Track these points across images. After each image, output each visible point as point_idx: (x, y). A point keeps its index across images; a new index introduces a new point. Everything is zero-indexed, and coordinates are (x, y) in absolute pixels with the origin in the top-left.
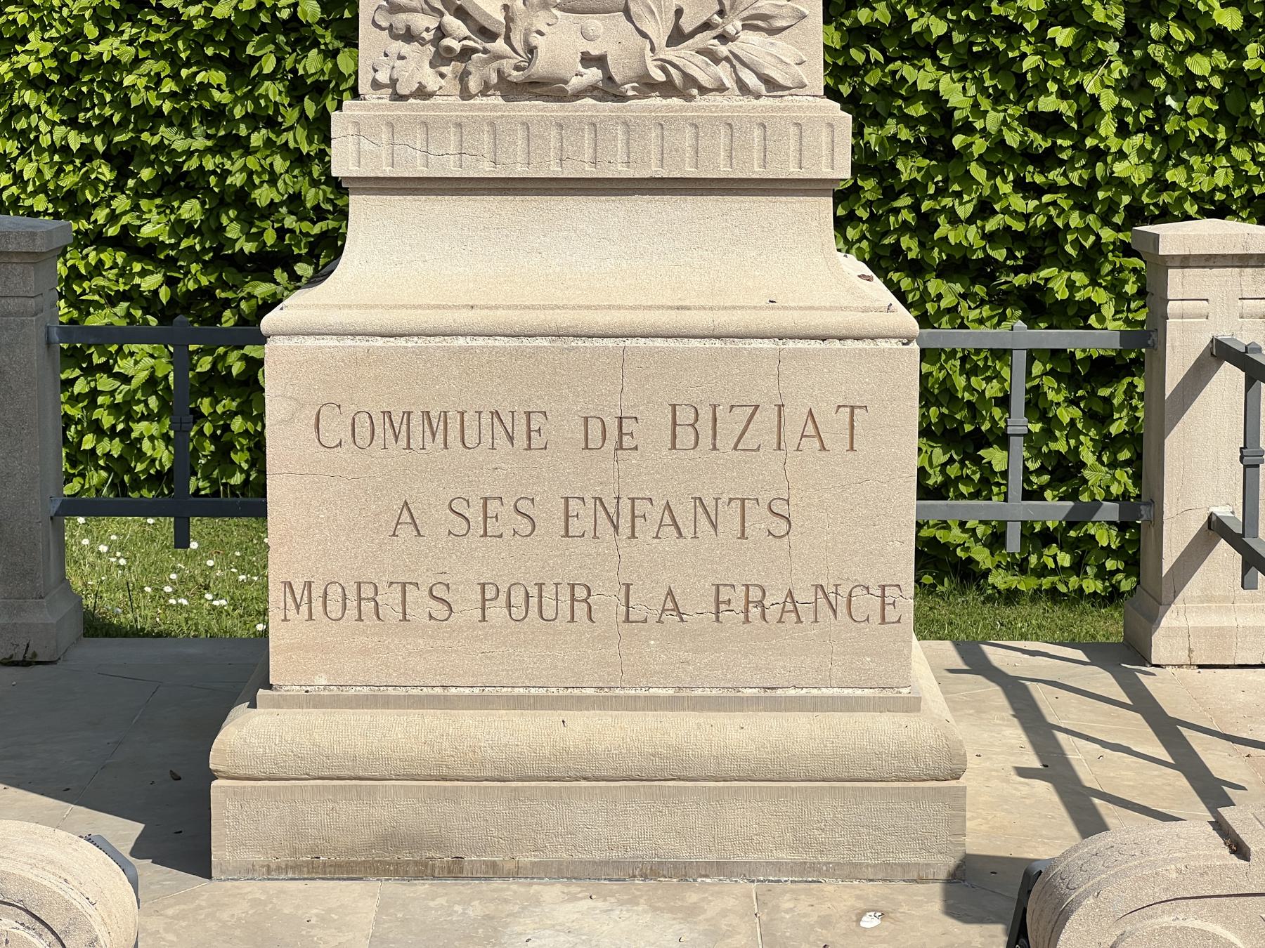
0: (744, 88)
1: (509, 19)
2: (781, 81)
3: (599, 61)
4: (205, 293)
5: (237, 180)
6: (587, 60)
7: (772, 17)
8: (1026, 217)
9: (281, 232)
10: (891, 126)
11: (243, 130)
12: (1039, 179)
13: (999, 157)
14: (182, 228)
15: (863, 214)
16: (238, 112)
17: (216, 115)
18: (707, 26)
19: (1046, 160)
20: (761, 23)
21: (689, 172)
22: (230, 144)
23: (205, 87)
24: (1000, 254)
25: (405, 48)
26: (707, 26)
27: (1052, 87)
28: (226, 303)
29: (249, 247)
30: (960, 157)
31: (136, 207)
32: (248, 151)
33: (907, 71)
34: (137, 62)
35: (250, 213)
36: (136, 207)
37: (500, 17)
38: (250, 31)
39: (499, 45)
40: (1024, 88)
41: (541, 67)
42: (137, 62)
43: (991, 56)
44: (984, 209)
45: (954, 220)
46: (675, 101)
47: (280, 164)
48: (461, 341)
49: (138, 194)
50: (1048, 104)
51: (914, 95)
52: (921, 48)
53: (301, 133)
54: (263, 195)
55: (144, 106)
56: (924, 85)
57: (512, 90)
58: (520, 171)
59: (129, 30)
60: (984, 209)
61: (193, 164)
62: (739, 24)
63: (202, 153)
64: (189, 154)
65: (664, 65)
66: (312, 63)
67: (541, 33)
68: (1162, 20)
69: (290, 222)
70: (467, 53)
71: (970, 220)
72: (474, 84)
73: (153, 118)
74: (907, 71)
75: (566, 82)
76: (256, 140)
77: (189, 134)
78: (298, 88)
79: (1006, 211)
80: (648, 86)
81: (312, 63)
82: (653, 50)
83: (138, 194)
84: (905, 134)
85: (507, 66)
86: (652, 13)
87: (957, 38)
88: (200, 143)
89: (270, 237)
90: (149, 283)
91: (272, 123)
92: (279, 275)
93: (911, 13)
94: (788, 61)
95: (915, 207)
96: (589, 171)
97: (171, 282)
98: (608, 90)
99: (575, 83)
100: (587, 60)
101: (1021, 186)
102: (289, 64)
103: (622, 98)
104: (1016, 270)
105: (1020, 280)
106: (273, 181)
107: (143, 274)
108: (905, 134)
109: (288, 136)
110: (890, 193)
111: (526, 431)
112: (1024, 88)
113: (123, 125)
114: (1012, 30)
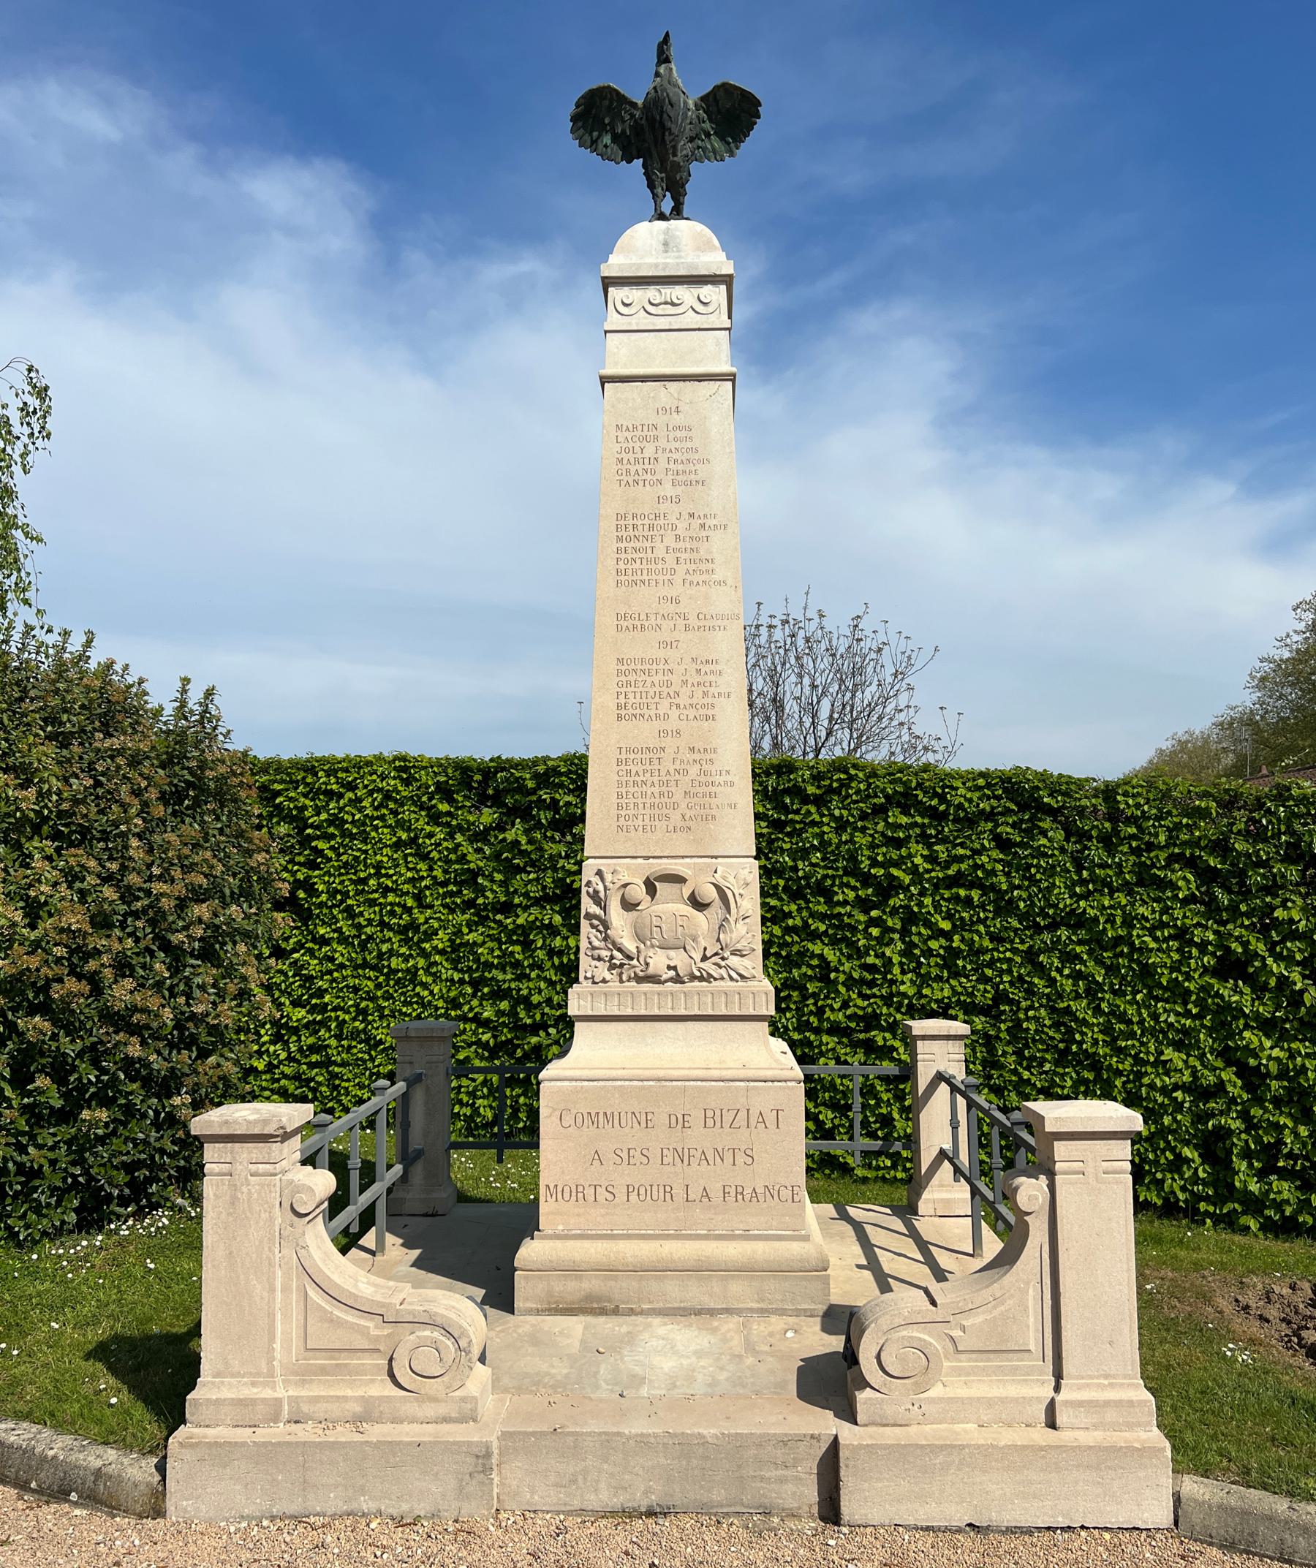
0: (731, 978)
1: (639, 952)
3: (675, 968)
4: (509, 1041)
5: (525, 992)
6: (669, 968)
8: (864, 1009)
9: (543, 1014)
10: (804, 969)
11: (528, 971)
12: (869, 992)
13: (850, 983)
14: (500, 1013)
15: (793, 1006)
16: (526, 963)
17: (517, 964)
18: (716, 954)
19: (871, 984)
21: (710, 1012)
22: (522, 977)
23: (512, 953)
24: (853, 1025)
25: (596, 963)
26: (716, 954)
27: (872, 953)
28: (518, 1046)
29: (529, 1021)
30: (835, 982)
31: (481, 1004)
32: (530, 980)
33: (810, 946)
34: (484, 943)
35: (530, 1007)
36: (481, 1004)
37: (635, 951)
38: (531, 929)
39: (635, 962)
40: (861, 954)
41: (651, 971)
42: (484, 943)
43: (845, 939)
44: (845, 1005)
45: (832, 1009)
46: (704, 984)
47: (543, 985)
48: (619, 1083)
49: (482, 999)
50: (870, 960)
51: (813, 956)
52: (815, 936)
53: (552, 972)
54: (536, 999)
55: (487, 961)
56: (817, 952)
57: (639, 980)
58: (643, 1012)
59: (481, 929)
60: (845, 1005)
61: (506, 985)
63: (510, 981)
64: (505, 981)
66: (558, 942)
68: (917, 926)
69: (547, 1010)
70: (622, 965)
71: (840, 1010)
72: (624, 978)
73: (489, 966)
74: (810, 946)
76: (533, 975)
77: (505, 973)
78: (551, 953)
79: (855, 1006)
80: (693, 978)
81: (558, 942)
83: (482, 999)
84: (810, 973)
85: (638, 970)
87: (830, 932)
88: (509, 976)
89: (538, 1017)
90: (485, 1038)
91: (541, 968)
92: (542, 1033)
93: (810, 921)
95: (815, 1004)
96: (670, 1012)
97: (495, 1037)
98: (678, 979)
99: (664, 977)
100: (669, 968)
101: (860, 995)
102: (548, 942)
104: (861, 1032)
105: (862, 1036)
106: (540, 992)
107: (483, 1033)
108: (810, 973)
109: (547, 973)
110: (805, 997)
111: (646, 1121)
112: (861, 954)
113: (477, 969)
114: (853, 929)
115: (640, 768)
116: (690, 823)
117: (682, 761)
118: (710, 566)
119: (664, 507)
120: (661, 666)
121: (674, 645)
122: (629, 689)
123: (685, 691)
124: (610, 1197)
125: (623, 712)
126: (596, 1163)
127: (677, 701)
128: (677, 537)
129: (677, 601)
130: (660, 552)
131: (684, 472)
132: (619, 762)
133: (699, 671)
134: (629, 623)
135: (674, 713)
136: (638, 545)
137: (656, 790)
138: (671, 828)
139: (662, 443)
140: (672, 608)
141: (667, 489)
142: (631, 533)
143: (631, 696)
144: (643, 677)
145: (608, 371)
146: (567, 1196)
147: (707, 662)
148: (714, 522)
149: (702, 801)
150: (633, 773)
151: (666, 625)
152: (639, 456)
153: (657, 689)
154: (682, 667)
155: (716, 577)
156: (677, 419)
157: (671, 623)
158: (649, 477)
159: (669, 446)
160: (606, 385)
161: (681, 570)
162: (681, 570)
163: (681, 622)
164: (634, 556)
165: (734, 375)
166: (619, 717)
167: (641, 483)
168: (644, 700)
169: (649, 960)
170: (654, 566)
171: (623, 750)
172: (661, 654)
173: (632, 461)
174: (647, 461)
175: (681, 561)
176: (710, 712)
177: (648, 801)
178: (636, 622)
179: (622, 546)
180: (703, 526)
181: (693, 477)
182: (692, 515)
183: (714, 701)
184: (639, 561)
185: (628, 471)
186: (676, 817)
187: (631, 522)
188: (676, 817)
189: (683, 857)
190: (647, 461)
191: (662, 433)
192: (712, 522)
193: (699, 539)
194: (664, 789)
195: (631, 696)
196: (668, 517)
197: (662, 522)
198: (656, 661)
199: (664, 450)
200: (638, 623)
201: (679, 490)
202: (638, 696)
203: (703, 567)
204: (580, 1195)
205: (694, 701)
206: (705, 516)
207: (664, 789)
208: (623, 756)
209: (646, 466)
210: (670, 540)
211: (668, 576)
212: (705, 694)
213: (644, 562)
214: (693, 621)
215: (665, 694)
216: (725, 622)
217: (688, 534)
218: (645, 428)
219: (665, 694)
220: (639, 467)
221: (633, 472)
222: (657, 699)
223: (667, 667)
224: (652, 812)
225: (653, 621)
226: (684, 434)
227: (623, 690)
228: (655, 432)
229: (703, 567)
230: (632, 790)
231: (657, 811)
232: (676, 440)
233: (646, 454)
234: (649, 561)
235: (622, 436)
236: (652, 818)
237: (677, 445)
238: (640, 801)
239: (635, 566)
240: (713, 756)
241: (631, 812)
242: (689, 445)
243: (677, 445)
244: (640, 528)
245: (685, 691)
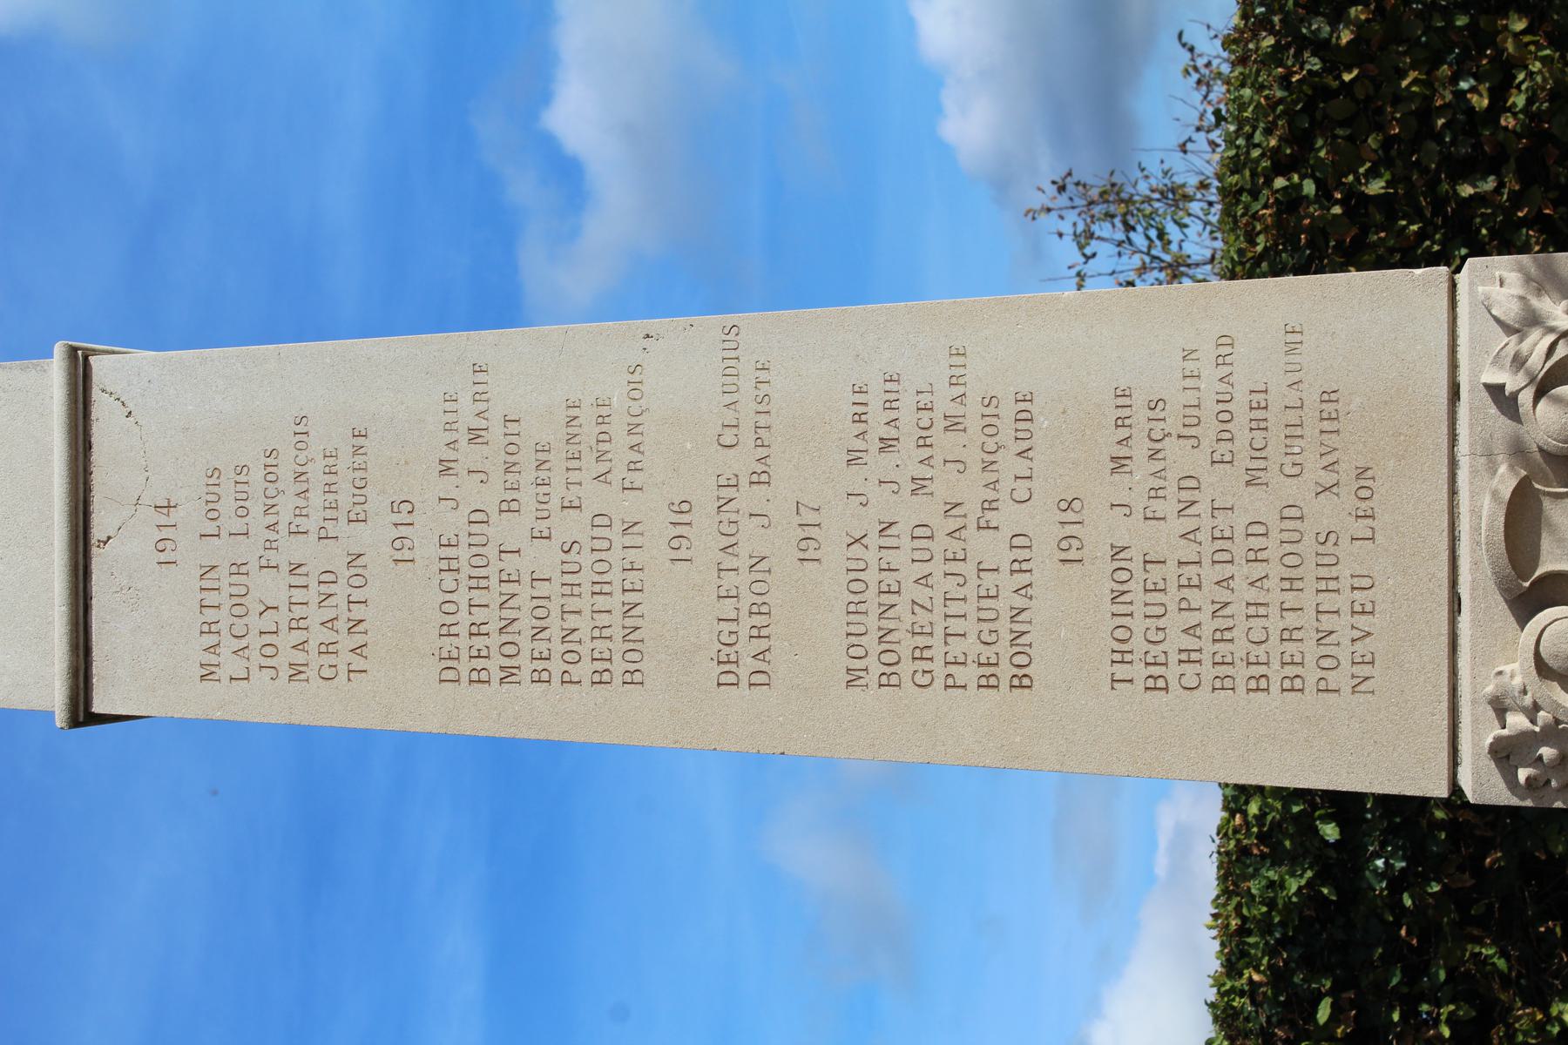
115: (1176, 621)
116: (1346, 471)
117: (1155, 494)
118: (587, 415)
119: (426, 551)
120: (872, 556)
121: (810, 517)
122: (938, 652)
123: (945, 485)
125: (1005, 671)
127: (972, 509)
128: (509, 508)
129: (682, 507)
130: (546, 559)
131: (329, 488)
132: (1156, 685)
133: (886, 444)
134: (747, 648)
135: (1009, 517)
136: (526, 623)
137: (1242, 571)
138: (1361, 528)
139: (249, 551)
140: (704, 524)
141: (374, 537)
142: (495, 640)
143: (957, 648)
144: (903, 609)
145: (55, 698)
147: (859, 419)
148: (465, 400)
149: (1276, 435)
150: (1188, 642)
151: (751, 538)
152: (283, 617)
153: (937, 568)
154: (875, 493)
155: (618, 398)
156: (190, 514)
157: (748, 526)
158: (341, 590)
159: (260, 534)
160: (98, 707)
161: (596, 498)
162: (596, 498)
163: (748, 498)
164: (555, 632)
165: (73, 351)
166: (1022, 682)
167: (358, 612)
168: (970, 608)
170: (585, 578)
171: (1121, 671)
172: (835, 554)
173: (297, 637)
174: (299, 596)
175: (572, 495)
176: (1008, 410)
177: (1275, 597)
178: (744, 632)
179: (527, 666)
180: (475, 435)
181: (344, 463)
182: (446, 468)
183: (974, 400)
184: (572, 622)
185: (327, 649)
186: (1327, 514)
187: (463, 642)
188: (1327, 514)
189: (1453, 492)
190: (299, 596)
191: (222, 552)
192: (466, 406)
193: (512, 449)
194: (1239, 548)
195: (957, 648)
196: (449, 535)
197: (463, 553)
198: (856, 573)
199: (270, 545)
200: (746, 622)
201: (377, 503)
202: (956, 626)
203: (589, 431)
205: (974, 457)
206: (449, 427)
207: (1239, 548)
208: (1139, 671)
209: (312, 595)
210: (505, 530)
211: (615, 534)
212: (954, 424)
213: (573, 604)
214: (742, 462)
215: (956, 546)
216: (746, 368)
217: (497, 477)
218: (211, 598)
219: (956, 546)
220: (316, 616)
221: (329, 636)
222: (968, 569)
223: (873, 540)
224: (1310, 585)
225: (743, 579)
226: (227, 489)
227: (938, 667)
228: (223, 571)
229: (589, 431)
230: (1240, 648)
231: (1309, 572)
232: (243, 512)
233: (280, 597)
234: (572, 589)
235: (231, 665)
236: (1327, 584)
237: (256, 508)
238: (1275, 624)
239: (584, 633)
240: (1139, 400)
241: (1311, 651)
242: (257, 475)
243: (256, 508)
244: (480, 615)
245: (945, 485)
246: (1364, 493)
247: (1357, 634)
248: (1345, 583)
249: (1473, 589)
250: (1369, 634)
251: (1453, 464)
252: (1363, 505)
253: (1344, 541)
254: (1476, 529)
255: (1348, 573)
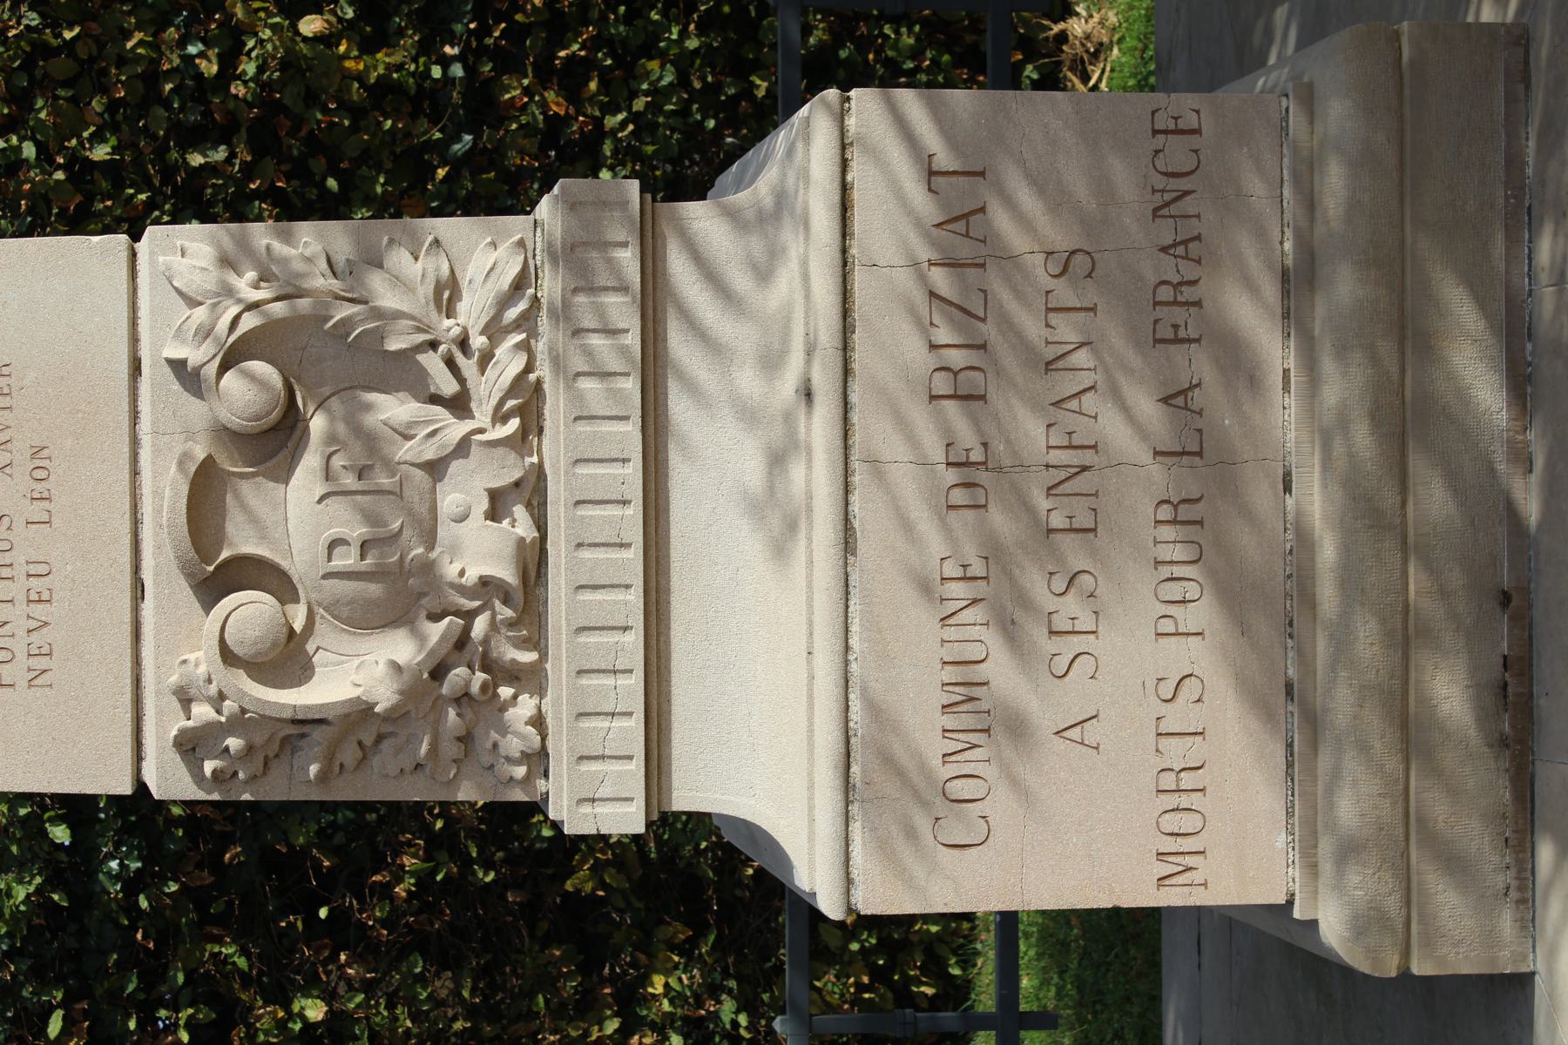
2: (517, 269)
7: (438, 282)
20: (446, 295)
41: (506, 573)
62: (448, 323)
65: (500, 417)
67: (462, 573)
75: (522, 540)
82: (481, 431)
86: (433, 433)
94: (491, 261)
100: (494, 514)
103: (539, 472)
124: (1190, 690)
126: (1092, 732)
138: (37, 511)
146: (1188, 822)
169: (472, 575)
189: (135, 473)
204: (1188, 780)
246: (40, 474)
247: (33, 624)
248: (20, 570)
249: (156, 575)
250: (46, 624)
251: (135, 442)
252: (39, 486)
253: (19, 525)
254: (158, 511)
255: (22, 560)
